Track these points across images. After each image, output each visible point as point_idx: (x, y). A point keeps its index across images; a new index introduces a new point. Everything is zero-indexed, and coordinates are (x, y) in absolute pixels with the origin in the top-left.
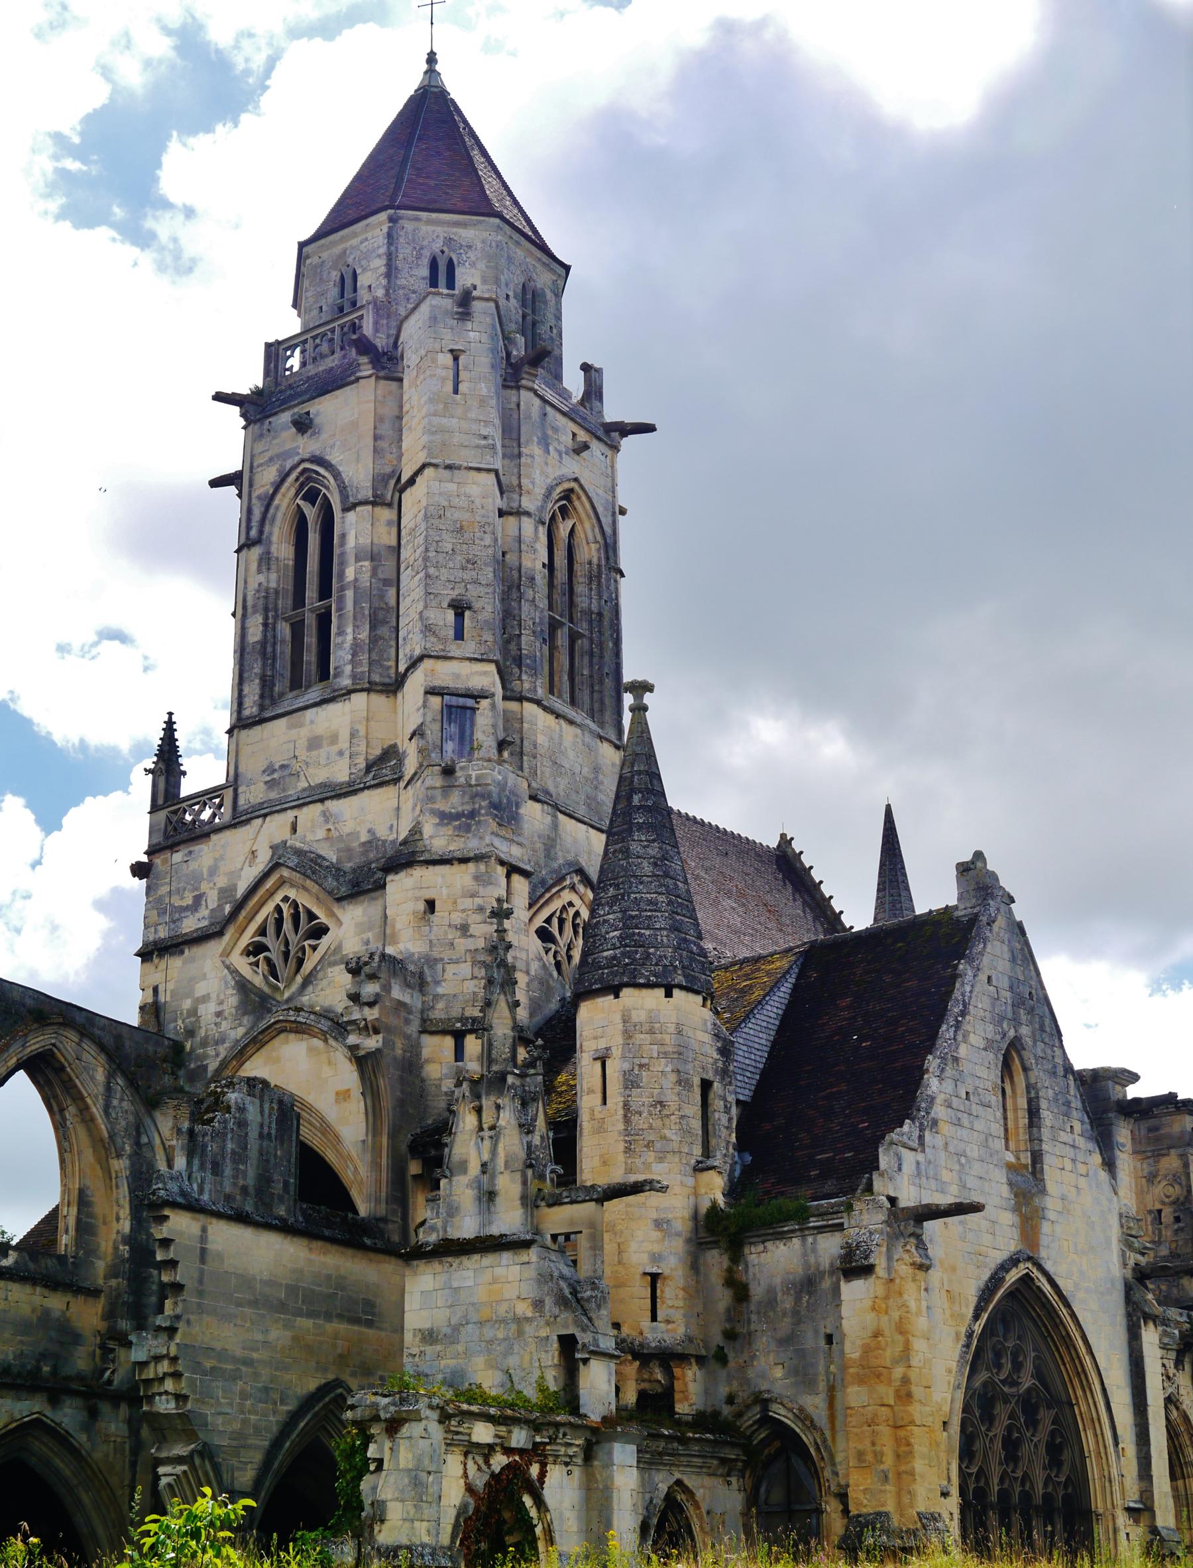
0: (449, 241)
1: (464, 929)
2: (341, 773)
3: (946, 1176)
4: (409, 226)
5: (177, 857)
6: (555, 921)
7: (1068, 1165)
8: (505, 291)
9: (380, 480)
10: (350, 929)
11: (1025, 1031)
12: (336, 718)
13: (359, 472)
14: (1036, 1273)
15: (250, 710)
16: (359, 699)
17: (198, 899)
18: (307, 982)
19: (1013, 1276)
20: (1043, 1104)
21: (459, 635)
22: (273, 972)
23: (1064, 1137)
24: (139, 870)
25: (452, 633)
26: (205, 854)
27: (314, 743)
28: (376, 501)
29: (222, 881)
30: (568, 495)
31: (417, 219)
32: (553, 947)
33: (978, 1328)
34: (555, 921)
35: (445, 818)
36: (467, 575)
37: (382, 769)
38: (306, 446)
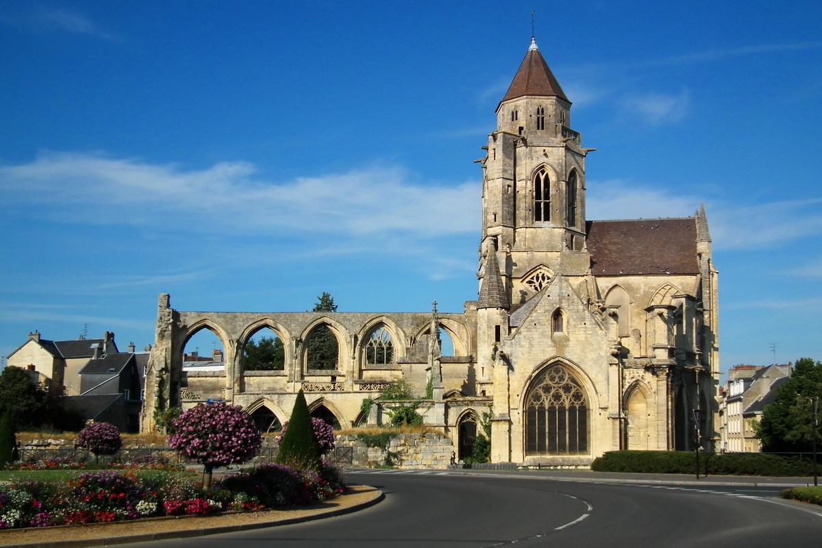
0: (516, 106)
3: (523, 344)
4: (507, 105)
6: (535, 278)
7: (582, 332)
8: (529, 114)
11: (564, 305)
14: (562, 360)
19: (552, 361)
20: (571, 320)
21: (495, 221)
23: (580, 326)
25: (493, 220)
30: (543, 167)
31: (508, 103)
32: (533, 284)
33: (534, 375)
34: (535, 278)
36: (497, 205)
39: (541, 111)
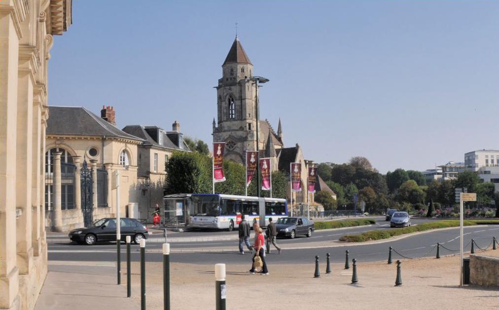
1: (252, 147)
2: (236, 128)
5: (217, 134)
9: (239, 97)
10: (239, 144)
12: (235, 122)
13: (237, 96)
15: (225, 120)
16: (238, 121)
17: (220, 139)
18: (234, 149)
22: (229, 147)
24: (212, 134)
26: (221, 134)
27: (233, 125)
28: (239, 100)
29: (223, 137)
35: (250, 136)
37: (242, 129)
38: (230, 92)
39: (250, 71)
